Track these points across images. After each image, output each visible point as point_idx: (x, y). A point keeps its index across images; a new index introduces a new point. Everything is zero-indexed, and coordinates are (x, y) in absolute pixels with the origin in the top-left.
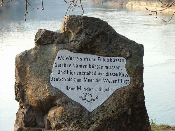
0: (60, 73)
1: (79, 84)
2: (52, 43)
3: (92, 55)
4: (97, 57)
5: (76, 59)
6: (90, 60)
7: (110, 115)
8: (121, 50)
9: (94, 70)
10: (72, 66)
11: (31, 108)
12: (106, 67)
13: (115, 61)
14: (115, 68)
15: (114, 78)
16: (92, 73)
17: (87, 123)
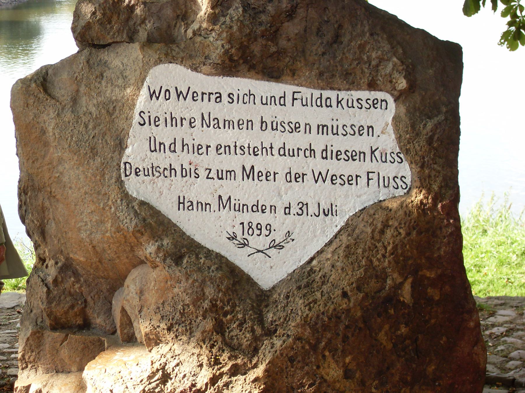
0: (156, 147)
1: (227, 188)
2: (131, 40)
4: (288, 89)
5: (213, 97)
6: (264, 102)
8: (377, 66)
9: (277, 139)
10: (198, 123)
12: (323, 126)
13: (355, 104)
17: (253, 331)
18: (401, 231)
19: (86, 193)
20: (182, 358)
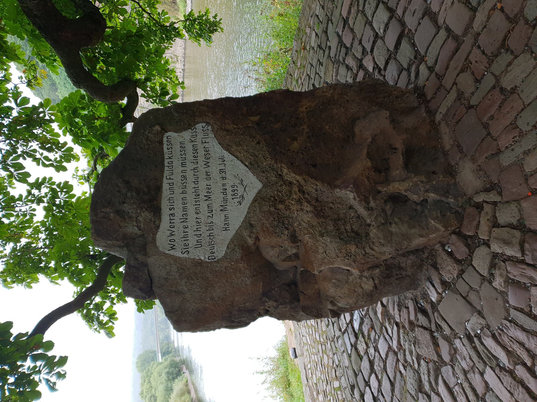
1: (216, 206)
2: (146, 265)
4: (165, 182)
7: (265, 148)
8: (150, 141)
9: (190, 186)
10: (185, 224)
11: (266, 294)
13: (170, 150)
14: (182, 149)
17: (281, 186)
19: (227, 281)
20: (300, 219)
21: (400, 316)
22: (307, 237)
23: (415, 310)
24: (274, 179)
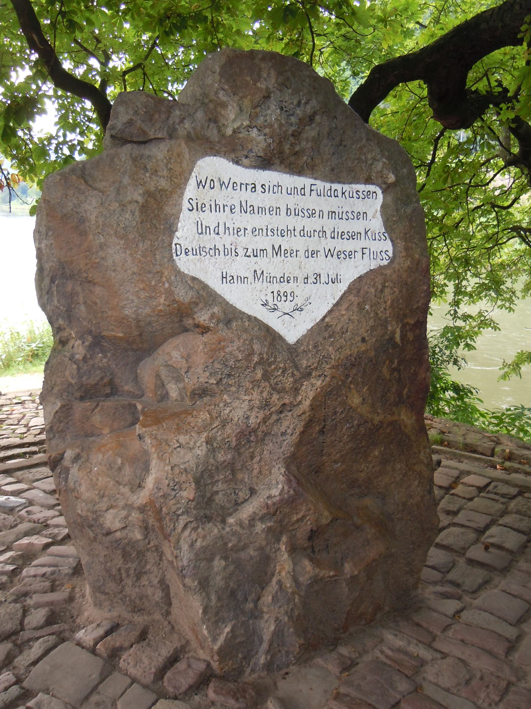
0: (202, 230)
3: (296, 177)
5: (249, 187)
6: (289, 192)
8: (371, 165)
9: (298, 223)
14: (355, 215)
15: (348, 246)
16: (294, 230)
17: (293, 375)
18: (395, 289)
20: (234, 405)
21: (35, 576)
22: (204, 416)
23: (51, 603)
24: (304, 363)
